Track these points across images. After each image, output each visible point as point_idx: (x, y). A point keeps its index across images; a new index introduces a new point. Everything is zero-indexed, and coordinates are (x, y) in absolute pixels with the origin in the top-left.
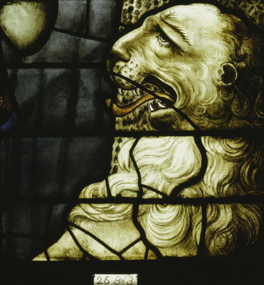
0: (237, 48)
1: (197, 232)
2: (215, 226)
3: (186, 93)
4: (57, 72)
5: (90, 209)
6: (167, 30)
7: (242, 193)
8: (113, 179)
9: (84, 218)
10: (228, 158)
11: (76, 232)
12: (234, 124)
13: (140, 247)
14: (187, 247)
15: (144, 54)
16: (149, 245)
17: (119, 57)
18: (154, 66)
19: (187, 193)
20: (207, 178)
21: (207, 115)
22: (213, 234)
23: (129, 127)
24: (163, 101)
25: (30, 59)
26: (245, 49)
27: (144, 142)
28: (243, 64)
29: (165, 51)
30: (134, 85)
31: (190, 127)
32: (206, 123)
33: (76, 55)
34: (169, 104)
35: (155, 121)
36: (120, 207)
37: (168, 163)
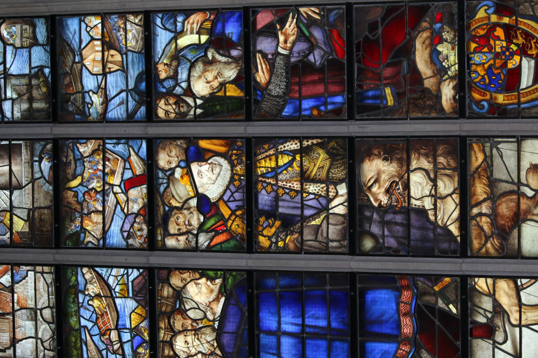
0: (376, 155)
1: (448, 172)
2: (445, 164)
3: (393, 176)
4: (386, 230)
5: (439, 217)
6: (369, 184)
7: (432, 153)
8: (427, 207)
9: (442, 220)
10: (418, 159)
11: (448, 223)
12: (405, 156)
13: (454, 196)
14: (454, 176)
15: (378, 194)
16: (453, 193)
17: (380, 204)
18: (383, 190)
19: (432, 176)
20: (426, 168)
21: (401, 168)
22: (449, 165)
23: (407, 200)
24: (396, 186)
25: (381, 241)
26: (376, 152)
27: (412, 194)
28: (382, 153)
29: (377, 185)
30: (390, 198)
31: (406, 175)
32: (405, 168)
33: (380, 222)
34: (397, 184)
35: (404, 190)
36: (438, 205)
37: (420, 184)
